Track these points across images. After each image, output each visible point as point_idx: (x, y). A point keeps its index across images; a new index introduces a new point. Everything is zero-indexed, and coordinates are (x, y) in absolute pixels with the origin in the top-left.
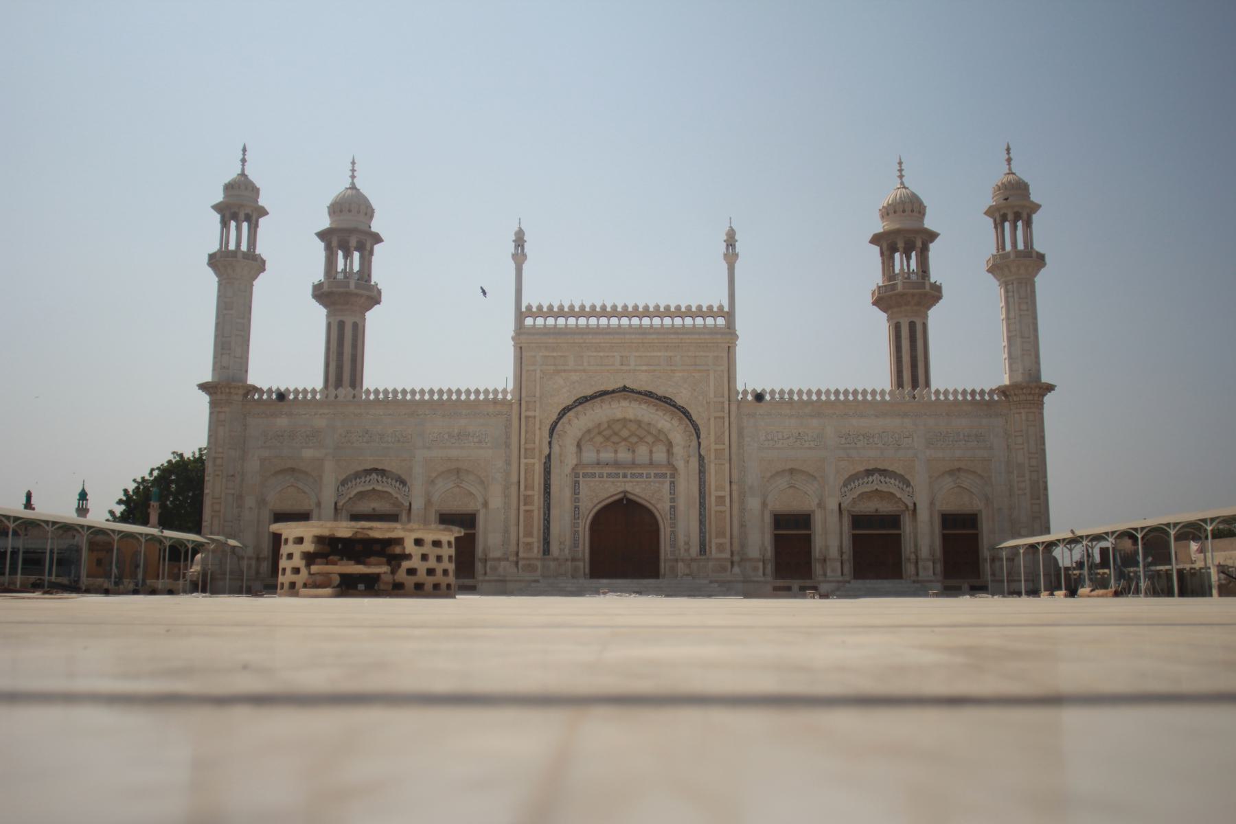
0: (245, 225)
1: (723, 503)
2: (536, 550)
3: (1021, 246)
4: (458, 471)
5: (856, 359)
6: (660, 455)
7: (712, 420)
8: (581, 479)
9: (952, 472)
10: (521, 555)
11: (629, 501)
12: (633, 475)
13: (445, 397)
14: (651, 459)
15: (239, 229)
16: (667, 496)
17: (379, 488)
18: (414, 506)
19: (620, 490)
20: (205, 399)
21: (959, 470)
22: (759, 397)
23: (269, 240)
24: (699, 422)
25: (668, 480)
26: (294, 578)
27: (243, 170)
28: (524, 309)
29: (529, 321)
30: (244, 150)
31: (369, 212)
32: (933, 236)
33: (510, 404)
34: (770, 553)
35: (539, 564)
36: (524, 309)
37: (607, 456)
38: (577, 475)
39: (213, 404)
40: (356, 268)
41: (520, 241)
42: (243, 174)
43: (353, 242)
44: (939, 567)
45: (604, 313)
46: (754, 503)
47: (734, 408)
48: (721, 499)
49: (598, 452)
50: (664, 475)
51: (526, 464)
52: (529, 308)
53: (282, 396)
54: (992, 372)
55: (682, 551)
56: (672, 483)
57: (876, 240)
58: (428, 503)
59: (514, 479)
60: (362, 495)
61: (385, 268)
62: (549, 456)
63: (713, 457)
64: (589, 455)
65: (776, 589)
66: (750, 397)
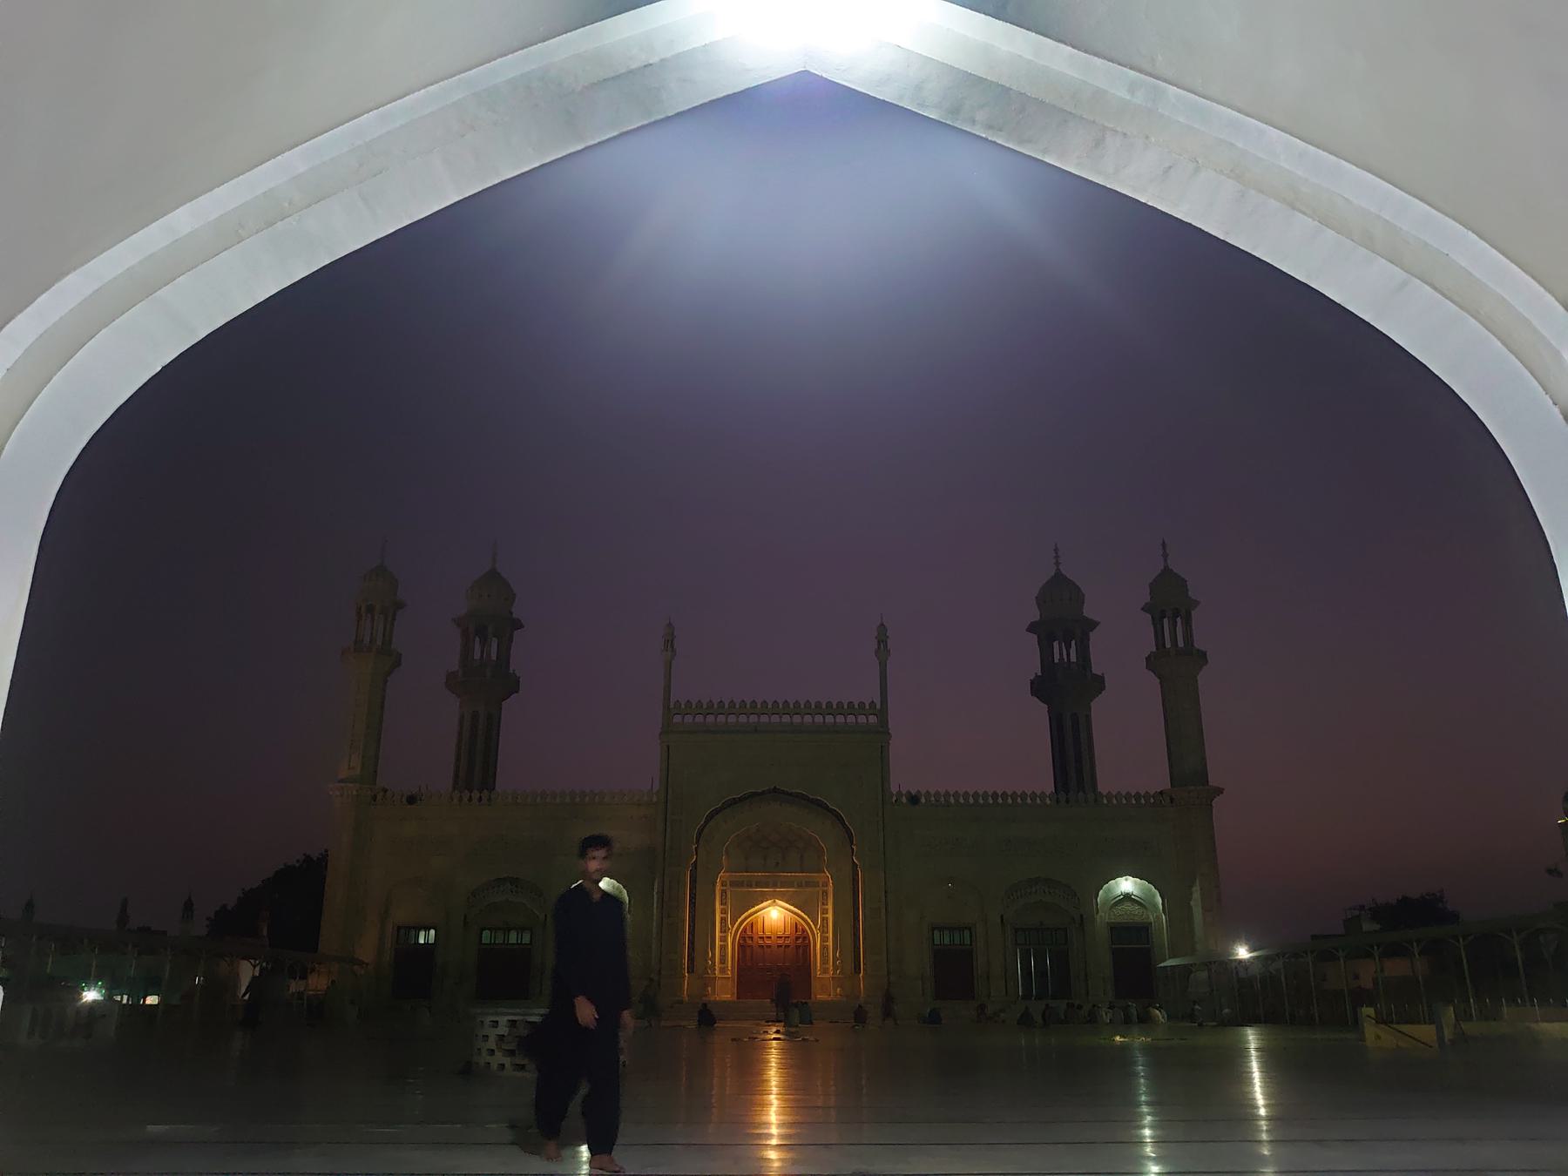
3: (1181, 644)
22: (914, 799)
26: (489, 1059)
29: (677, 719)
32: (1093, 625)
54: (1156, 778)
57: (1032, 628)
66: (904, 800)
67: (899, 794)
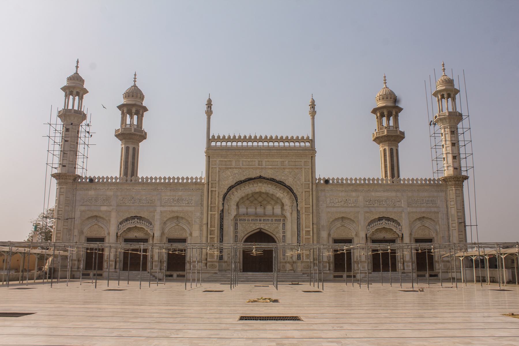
0: (77, 98)
1: (309, 235)
2: (216, 258)
4: (177, 217)
5: (368, 164)
6: (278, 210)
7: (304, 192)
8: (238, 222)
9: (419, 219)
10: (208, 260)
11: (262, 232)
12: (264, 220)
13: (171, 181)
14: (273, 212)
15: (74, 100)
16: (281, 231)
17: (138, 226)
18: (155, 235)
19: (258, 227)
20: (54, 181)
21: (423, 217)
22: (327, 181)
23: (88, 104)
24: (297, 194)
25: (282, 222)
27: (77, 71)
28: (211, 138)
29: (213, 144)
30: (78, 62)
31: (142, 97)
33: (203, 184)
34: (332, 259)
35: (217, 264)
36: (211, 138)
37: (251, 210)
38: (236, 220)
39: (59, 184)
40: (135, 123)
41: (209, 104)
42: (77, 73)
43: (134, 110)
44: (415, 265)
45: (250, 139)
46: (324, 234)
47: (314, 186)
48: (308, 232)
49: (247, 208)
50: (280, 220)
51: (211, 214)
52: (213, 136)
53: (91, 180)
55: (289, 258)
56: (284, 224)
58: (163, 234)
59: (205, 221)
60: (129, 229)
61: (148, 123)
62: (223, 210)
63: (304, 211)
64: (243, 210)
65: (335, 277)
66: (322, 182)
67: (320, 179)
